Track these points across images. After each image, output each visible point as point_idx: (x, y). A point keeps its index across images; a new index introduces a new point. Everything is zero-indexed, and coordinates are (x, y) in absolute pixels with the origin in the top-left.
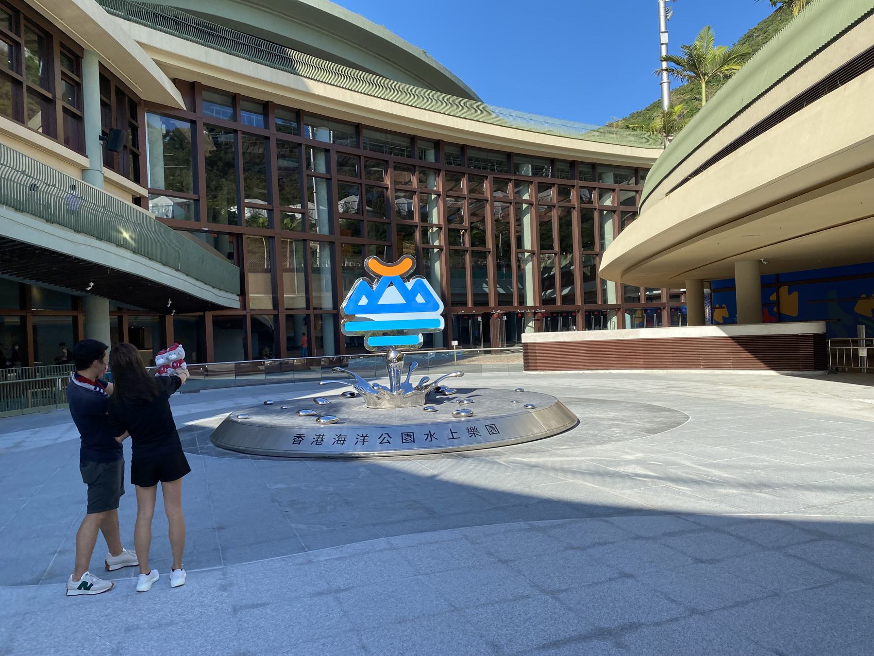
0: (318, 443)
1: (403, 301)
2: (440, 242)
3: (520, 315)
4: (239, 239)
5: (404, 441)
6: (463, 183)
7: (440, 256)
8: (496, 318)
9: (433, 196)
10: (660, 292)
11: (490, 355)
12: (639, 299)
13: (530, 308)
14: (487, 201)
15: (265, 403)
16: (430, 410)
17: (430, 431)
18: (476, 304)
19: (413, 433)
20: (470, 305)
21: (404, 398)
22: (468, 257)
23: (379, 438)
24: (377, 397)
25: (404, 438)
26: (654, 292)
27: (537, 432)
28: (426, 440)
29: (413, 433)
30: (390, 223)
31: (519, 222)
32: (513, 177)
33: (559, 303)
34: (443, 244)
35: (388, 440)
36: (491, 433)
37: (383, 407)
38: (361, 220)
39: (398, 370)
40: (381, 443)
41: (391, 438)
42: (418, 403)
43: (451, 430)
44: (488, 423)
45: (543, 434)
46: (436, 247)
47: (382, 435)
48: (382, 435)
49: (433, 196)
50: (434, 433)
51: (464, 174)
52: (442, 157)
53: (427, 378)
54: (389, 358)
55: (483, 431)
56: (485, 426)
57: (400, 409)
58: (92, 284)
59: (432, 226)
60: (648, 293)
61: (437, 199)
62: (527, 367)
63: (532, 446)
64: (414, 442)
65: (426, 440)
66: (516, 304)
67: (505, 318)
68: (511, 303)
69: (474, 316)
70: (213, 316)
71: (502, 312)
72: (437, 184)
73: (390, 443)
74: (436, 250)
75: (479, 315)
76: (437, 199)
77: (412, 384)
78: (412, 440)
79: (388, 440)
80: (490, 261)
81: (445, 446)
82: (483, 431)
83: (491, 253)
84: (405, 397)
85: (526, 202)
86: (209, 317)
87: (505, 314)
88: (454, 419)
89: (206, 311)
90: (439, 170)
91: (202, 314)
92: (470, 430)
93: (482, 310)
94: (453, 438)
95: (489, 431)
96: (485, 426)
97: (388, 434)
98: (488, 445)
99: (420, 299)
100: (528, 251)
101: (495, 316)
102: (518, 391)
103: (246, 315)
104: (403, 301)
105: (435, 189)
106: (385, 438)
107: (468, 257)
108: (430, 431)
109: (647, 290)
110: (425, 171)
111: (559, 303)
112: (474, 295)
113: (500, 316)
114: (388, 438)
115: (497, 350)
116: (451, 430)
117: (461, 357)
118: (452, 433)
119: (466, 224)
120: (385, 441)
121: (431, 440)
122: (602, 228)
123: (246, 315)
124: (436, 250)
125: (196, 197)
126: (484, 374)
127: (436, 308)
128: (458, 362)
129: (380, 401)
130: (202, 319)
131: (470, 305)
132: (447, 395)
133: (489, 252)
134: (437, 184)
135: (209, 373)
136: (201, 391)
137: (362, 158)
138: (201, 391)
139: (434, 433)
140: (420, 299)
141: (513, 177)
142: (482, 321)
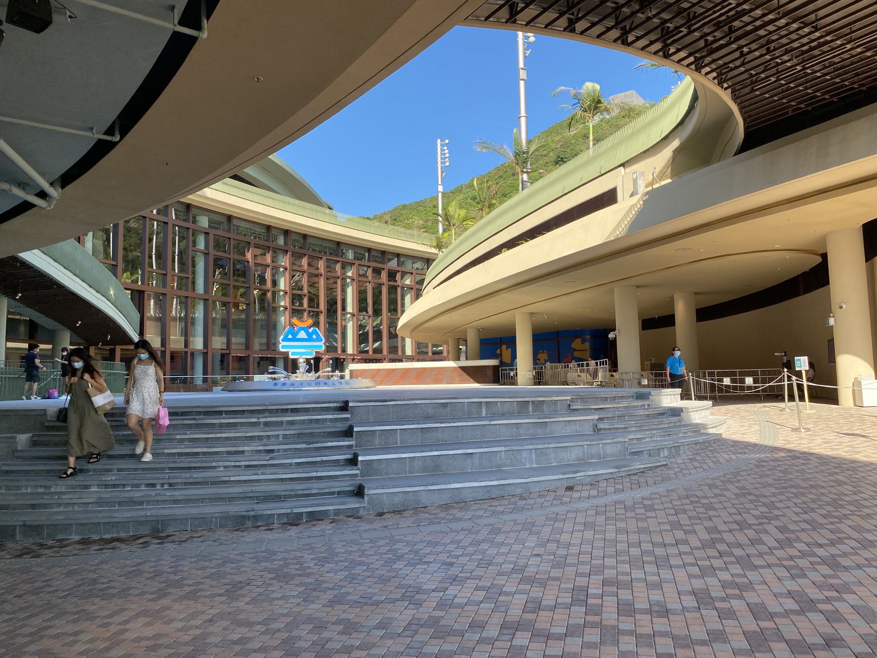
1: (307, 337)
2: (285, 303)
3: (342, 360)
6: (304, 262)
7: (285, 313)
9: (282, 269)
10: (442, 348)
12: (427, 353)
13: (350, 355)
14: (321, 275)
26: (439, 348)
31: (344, 291)
32: (341, 259)
33: (371, 353)
34: (288, 305)
46: (283, 306)
49: (282, 269)
51: (305, 255)
52: (290, 242)
58: (80, 322)
59: (280, 291)
60: (435, 349)
61: (284, 272)
66: (339, 352)
68: (336, 351)
72: (285, 261)
74: (282, 309)
76: (284, 272)
80: (322, 318)
83: (323, 313)
85: (349, 277)
87: (331, 359)
90: (287, 251)
91: (113, 347)
99: (314, 337)
100: (350, 313)
101: (324, 360)
104: (307, 337)
105: (283, 264)
109: (434, 346)
110: (276, 251)
111: (371, 353)
113: (327, 360)
119: (305, 291)
122: (403, 299)
125: (114, 263)
127: (321, 340)
133: (322, 312)
134: (285, 261)
137: (232, 240)
140: (314, 337)
141: (341, 259)
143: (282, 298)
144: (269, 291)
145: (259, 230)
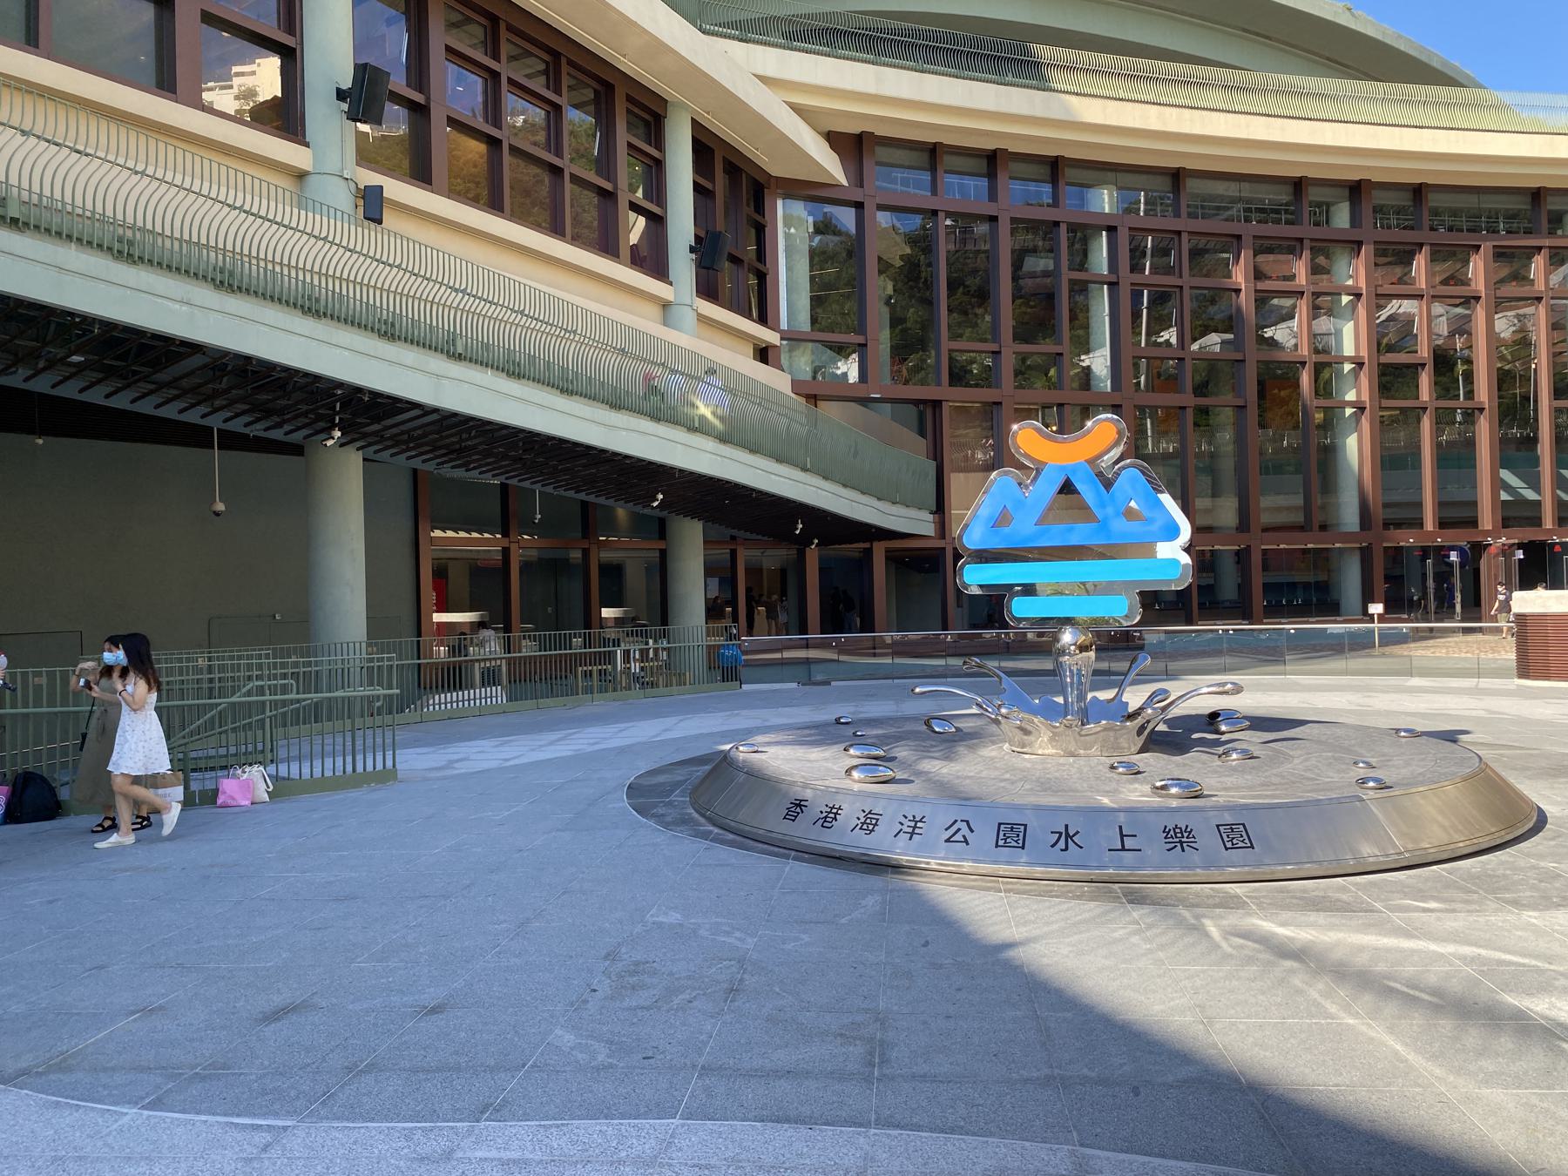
0: (825, 824)
2: (1359, 394)
4: (937, 410)
5: (1001, 843)
6: (1419, 263)
7: (1358, 421)
8: (1497, 555)
9: (1345, 299)
11: (1471, 638)
15: (838, 721)
16: (1121, 770)
17: (1067, 826)
18: (1443, 524)
19: (1025, 826)
20: (1429, 525)
21: (1081, 736)
22: (1426, 423)
23: (946, 829)
24: (1021, 728)
25: (1001, 836)
27: (1369, 852)
28: (1052, 846)
29: (1025, 826)
30: (1243, 361)
32: (1547, 242)
34: (1365, 397)
35: (964, 836)
36: (1229, 845)
37: (1040, 752)
38: (1058, 354)
39: (1079, 670)
40: (948, 841)
41: (972, 831)
42: (1118, 748)
43: (1120, 827)
44: (1228, 818)
45: (1391, 860)
46: (1351, 404)
47: (956, 821)
48: (956, 821)
49: (1345, 299)
50: (1078, 832)
51: (1421, 245)
52: (1367, 210)
53: (1165, 691)
54: (1059, 646)
55: (1208, 840)
56: (1218, 826)
57: (1071, 759)
58: (660, 497)
61: (1353, 306)
62: (1526, 668)
63: (1344, 889)
64: (1023, 847)
65: (1052, 846)
67: (1520, 555)
68: (1537, 521)
69: (1441, 553)
70: (887, 551)
71: (1512, 541)
72: (1353, 272)
73: (967, 844)
74: (1349, 411)
75: (1453, 548)
76: (1353, 306)
77: (1127, 703)
78: (1020, 842)
79: (964, 836)
80: (1484, 431)
81: (1098, 867)
82: (1208, 840)
83: (1486, 412)
84: (1083, 733)
86: (879, 550)
87: (1520, 546)
88: (1156, 800)
89: (874, 540)
90: (1360, 244)
91: (867, 545)
92: (1172, 833)
93: (1462, 538)
94: (1123, 849)
95: (1226, 839)
96: (1218, 826)
97: (967, 822)
98: (1215, 874)
101: (1493, 550)
102: (1403, 734)
103: (944, 548)
105: (1350, 282)
106: (959, 830)
107: (1426, 423)
108: (1067, 826)
110: (1323, 250)
112: (1441, 505)
113: (1507, 552)
114: (965, 830)
115: (1490, 627)
116: (1120, 827)
117: (1389, 640)
118: (1122, 836)
120: (958, 837)
121: (1066, 849)
123: (944, 548)
124: (1349, 411)
126: (1416, 681)
128: (1381, 650)
129: (1031, 738)
130: (868, 553)
131: (1429, 525)
132: (1223, 733)
133: (1481, 410)
134: (1353, 272)
135: (877, 651)
136: (833, 683)
137: (1185, 237)
138: (833, 683)
139: (1078, 832)
141: (1547, 242)
142: (1460, 563)
143: (1351, 379)
144: (1303, 364)
145: (1269, 195)
